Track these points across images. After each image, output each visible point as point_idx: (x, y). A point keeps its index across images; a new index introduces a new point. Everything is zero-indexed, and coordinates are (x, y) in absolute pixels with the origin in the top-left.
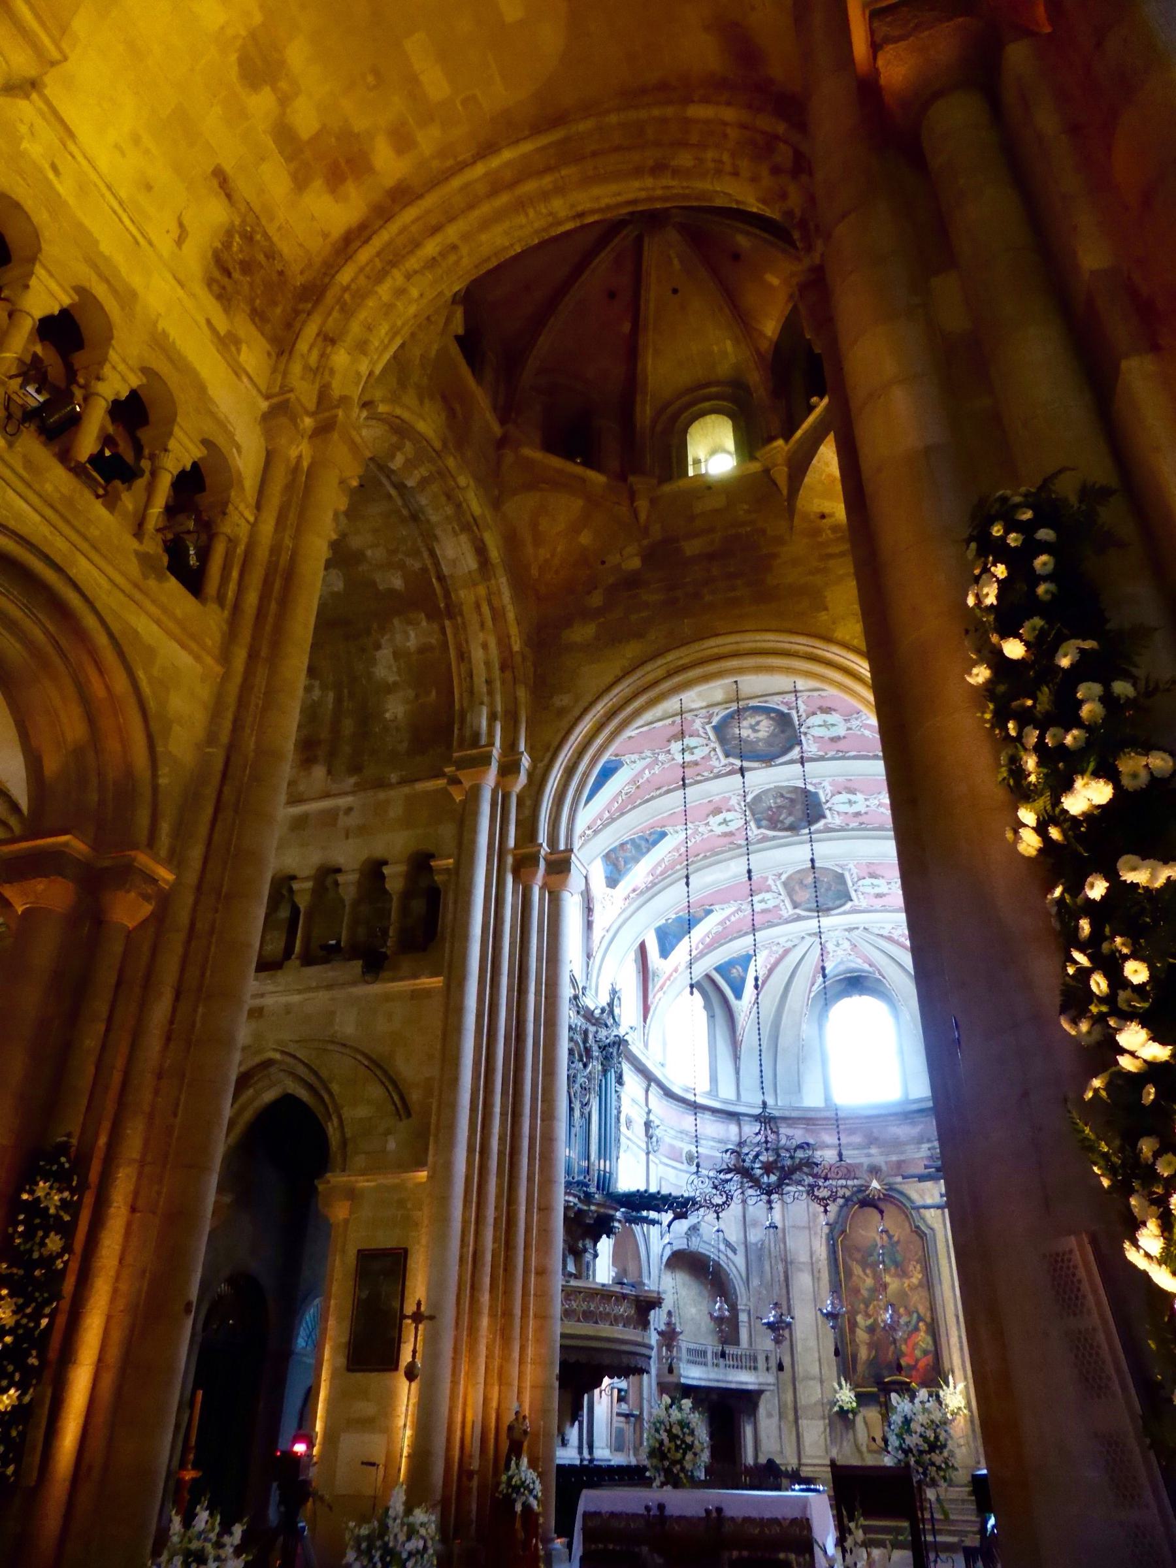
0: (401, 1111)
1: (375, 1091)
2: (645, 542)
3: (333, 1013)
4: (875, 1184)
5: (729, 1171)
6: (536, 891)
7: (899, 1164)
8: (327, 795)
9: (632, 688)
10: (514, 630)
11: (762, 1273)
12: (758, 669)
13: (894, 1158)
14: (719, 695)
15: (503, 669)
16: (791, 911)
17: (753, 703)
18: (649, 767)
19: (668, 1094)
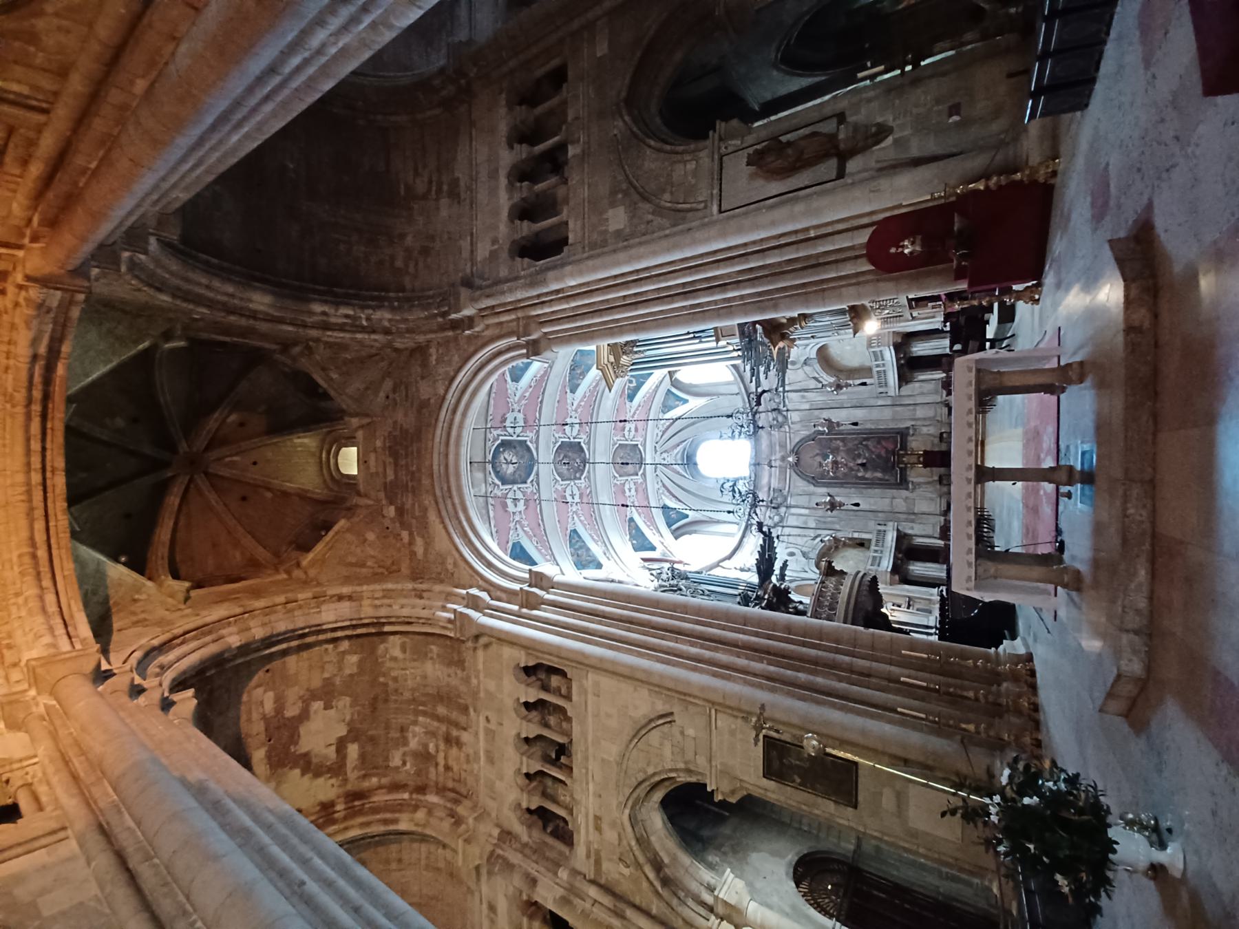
0: (669, 719)
1: (654, 737)
2: (384, 502)
3: (603, 760)
4: (790, 459)
5: (734, 491)
6: (547, 596)
7: (780, 446)
8: (477, 734)
9: (455, 522)
10: (399, 586)
11: (833, 523)
12: (458, 445)
13: (778, 448)
14: (480, 475)
15: (421, 597)
16: (639, 477)
17: (490, 457)
18: (522, 527)
19: (729, 557)
